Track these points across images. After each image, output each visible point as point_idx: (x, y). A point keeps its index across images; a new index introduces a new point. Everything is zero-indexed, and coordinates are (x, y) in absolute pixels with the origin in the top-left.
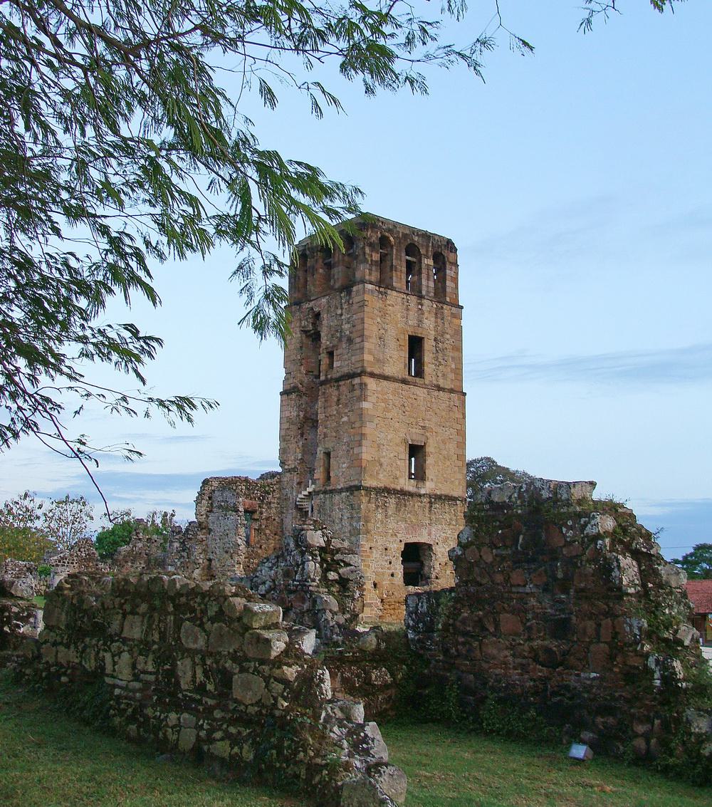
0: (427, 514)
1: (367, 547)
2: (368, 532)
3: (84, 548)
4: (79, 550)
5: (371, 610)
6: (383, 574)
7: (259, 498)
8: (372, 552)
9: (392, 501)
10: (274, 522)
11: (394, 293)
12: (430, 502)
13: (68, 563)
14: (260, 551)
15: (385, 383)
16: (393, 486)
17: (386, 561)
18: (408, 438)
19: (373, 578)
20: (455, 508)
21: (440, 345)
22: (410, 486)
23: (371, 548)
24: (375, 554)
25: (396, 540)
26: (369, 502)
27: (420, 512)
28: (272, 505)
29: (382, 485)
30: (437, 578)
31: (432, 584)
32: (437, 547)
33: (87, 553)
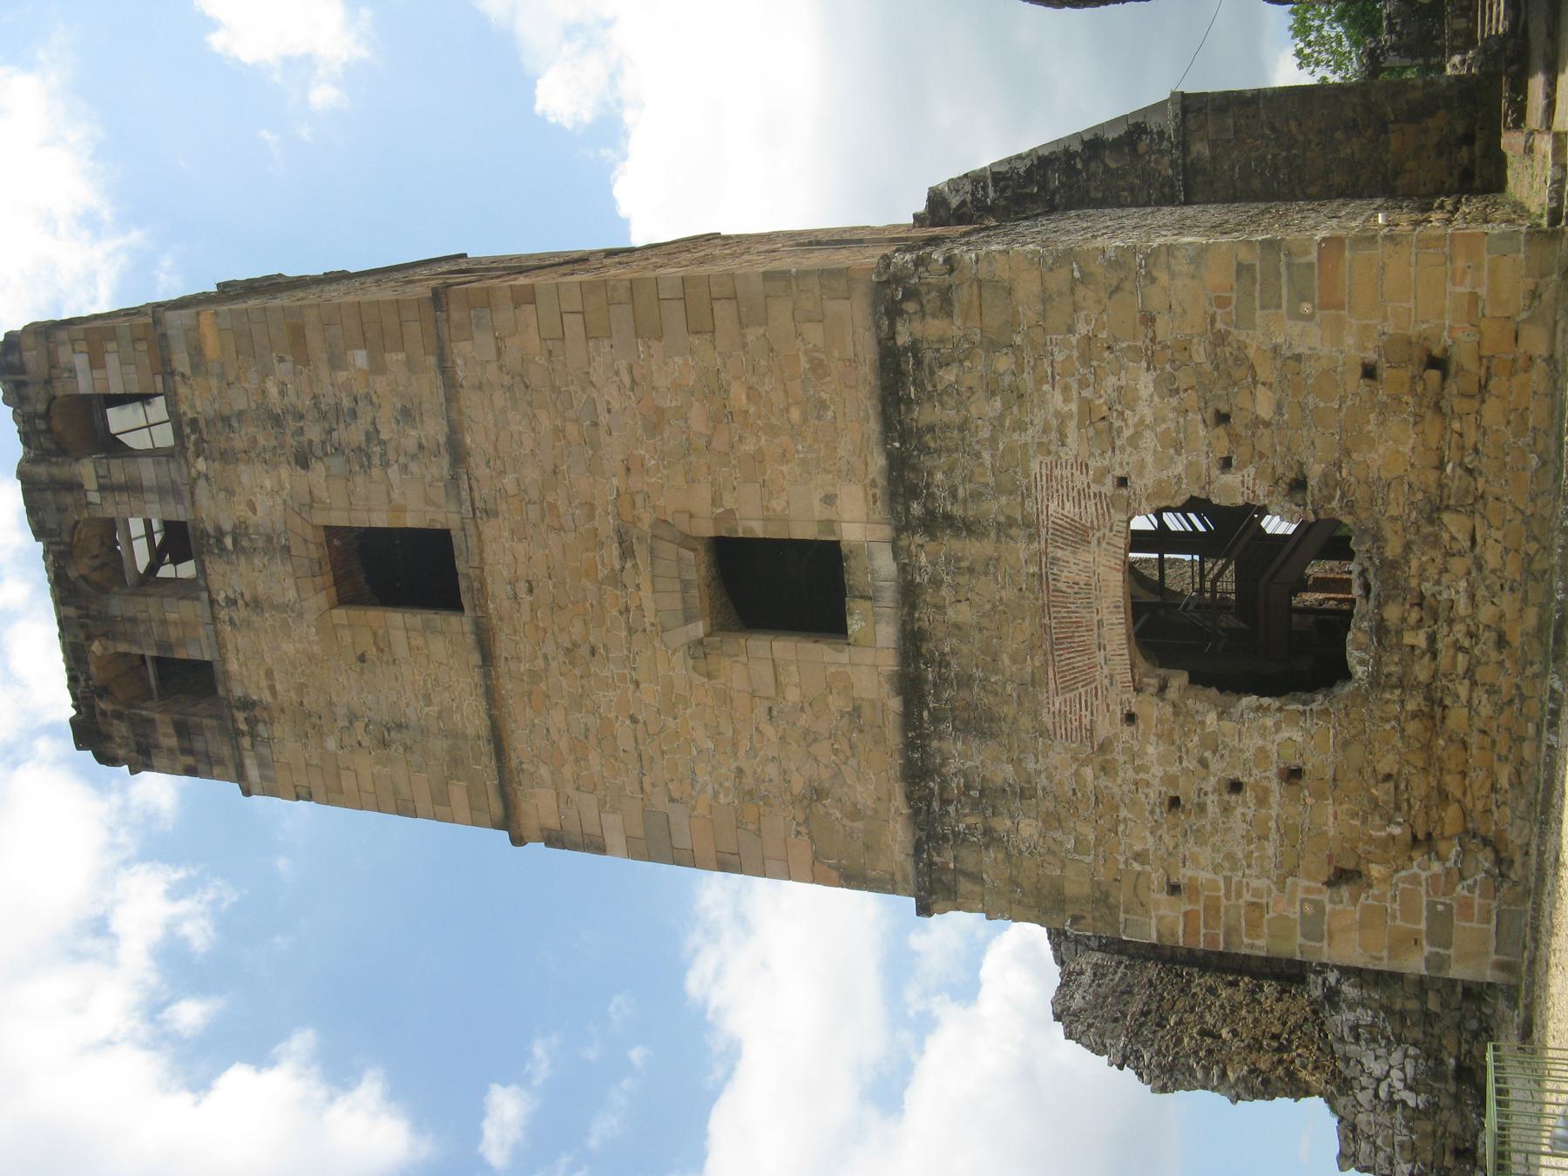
5: (1469, 918)
6: (1289, 832)
8: (1193, 890)
12: (933, 523)
15: (520, 744)
17: (1227, 810)
19: (1306, 885)
20: (929, 355)
21: (314, 433)
23: (1174, 889)
24: (1200, 871)
26: (976, 878)
29: (899, 790)
32: (1136, 483)
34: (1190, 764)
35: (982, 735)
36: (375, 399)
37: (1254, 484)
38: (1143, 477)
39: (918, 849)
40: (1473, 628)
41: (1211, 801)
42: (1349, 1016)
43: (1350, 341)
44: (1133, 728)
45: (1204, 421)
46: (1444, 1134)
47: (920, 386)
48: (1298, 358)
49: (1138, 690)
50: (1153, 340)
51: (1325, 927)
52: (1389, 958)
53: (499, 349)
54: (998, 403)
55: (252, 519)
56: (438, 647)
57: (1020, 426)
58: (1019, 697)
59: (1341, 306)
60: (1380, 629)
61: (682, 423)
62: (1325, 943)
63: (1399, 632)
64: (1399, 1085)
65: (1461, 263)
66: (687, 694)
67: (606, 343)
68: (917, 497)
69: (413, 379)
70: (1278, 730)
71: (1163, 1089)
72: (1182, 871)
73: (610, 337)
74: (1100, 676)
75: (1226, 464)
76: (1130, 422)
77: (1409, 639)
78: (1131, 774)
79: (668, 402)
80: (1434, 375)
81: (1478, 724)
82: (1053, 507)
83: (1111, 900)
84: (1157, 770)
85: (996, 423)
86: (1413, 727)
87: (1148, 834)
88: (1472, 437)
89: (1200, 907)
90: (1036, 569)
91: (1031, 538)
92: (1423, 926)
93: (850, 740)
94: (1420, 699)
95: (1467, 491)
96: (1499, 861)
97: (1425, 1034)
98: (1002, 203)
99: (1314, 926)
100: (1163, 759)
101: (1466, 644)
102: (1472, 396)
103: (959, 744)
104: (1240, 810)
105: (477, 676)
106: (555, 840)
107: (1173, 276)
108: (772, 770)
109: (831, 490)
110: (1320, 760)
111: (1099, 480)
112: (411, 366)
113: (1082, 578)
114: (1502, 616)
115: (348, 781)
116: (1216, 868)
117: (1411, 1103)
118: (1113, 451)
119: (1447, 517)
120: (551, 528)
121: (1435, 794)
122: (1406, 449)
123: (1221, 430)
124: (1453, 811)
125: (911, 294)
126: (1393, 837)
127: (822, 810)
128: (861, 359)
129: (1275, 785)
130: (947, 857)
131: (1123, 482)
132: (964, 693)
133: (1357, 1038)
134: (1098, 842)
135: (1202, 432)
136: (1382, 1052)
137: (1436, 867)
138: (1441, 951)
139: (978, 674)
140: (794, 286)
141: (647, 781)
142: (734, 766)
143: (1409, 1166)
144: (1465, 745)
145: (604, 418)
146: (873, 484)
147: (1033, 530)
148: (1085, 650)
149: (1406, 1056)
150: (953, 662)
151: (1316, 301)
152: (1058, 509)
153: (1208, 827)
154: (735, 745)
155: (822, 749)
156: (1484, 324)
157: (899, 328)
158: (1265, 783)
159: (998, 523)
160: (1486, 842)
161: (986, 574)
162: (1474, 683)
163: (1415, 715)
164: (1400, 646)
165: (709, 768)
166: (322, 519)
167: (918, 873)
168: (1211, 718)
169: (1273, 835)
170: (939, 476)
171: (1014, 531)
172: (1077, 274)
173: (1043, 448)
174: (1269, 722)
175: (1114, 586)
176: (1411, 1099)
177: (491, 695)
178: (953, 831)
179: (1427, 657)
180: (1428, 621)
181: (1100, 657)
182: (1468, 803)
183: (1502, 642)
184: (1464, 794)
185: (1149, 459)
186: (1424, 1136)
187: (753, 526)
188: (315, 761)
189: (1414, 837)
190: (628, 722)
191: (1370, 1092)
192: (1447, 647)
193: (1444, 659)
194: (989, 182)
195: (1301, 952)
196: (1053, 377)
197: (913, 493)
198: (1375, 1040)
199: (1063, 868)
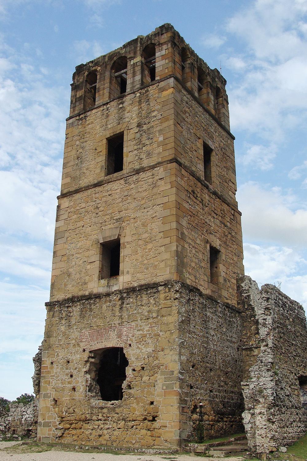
0: (118, 314)
6: (63, 389)
8: (52, 368)
9: (76, 310)
11: (94, 111)
12: (122, 298)
17: (67, 375)
19: (54, 394)
20: (156, 295)
21: (145, 127)
23: (52, 363)
24: (56, 369)
26: (53, 316)
27: (108, 314)
30: (129, 387)
32: (130, 349)
34: (76, 365)
36: (152, 144)
37: (129, 377)
38: (131, 350)
39: (58, 302)
40: (103, 429)
43: (158, 399)
44: (82, 352)
45: (142, 364)
46: (17, 427)
48: (155, 386)
49: (90, 352)
50: (158, 351)
51: (46, 399)
52: (41, 413)
53: (161, 179)
55: (126, 112)
56: (98, 170)
58: (88, 323)
60: (102, 408)
62: (43, 399)
65: (173, 424)
66: (89, 240)
68: (127, 295)
69: (156, 155)
70: (83, 385)
71: (34, 360)
74: (92, 343)
75: (134, 370)
76: (142, 346)
77: (100, 415)
79: (149, 228)
80: (151, 418)
81: (85, 431)
82: (125, 329)
85: (142, 313)
86: (83, 417)
87: (62, 356)
88: (139, 427)
90: (113, 326)
92: (47, 421)
93: (80, 282)
96: (60, 437)
98: (243, 298)
101: (100, 428)
102: (147, 428)
103: (78, 310)
104: (67, 378)
105: (92, 183)
106: (58, 207)
109: (130, 273)
111: (131, 340)
112: (159, 153)
113: (111, 337)
115: (70, 149)
116: (56, 373)
118: (136, 343)
120: (123, 199)
121: (71, 422)
122: (136, 413)
123: (140, 368)
124: (68, 426)
127: (66, 277)
128: (157, 278)
129: (72, 385)
130: (57, 308)
131: (130, 345)
132: (89, 310)
134: (61, 345)
135: (140, 364)
137: (58, 423)
138: (42, 425)
140: (173, 259)
143: (11, 420)
144: (81, 428)
145: (146, 210)
147: (120, 324)
148: (97, 339)
149: (31, 418)
151: (166, 390)
153: (64, 370)
154: (78, 253)
155: (78, 276)
157: (163, 287)
158: (72, 383)
160: (63, 434)
161: (112, 314)
162: (92, 430)
163: (86, 417)
164: (99, 413)
165: (74, 247)
166: (125, 133)
167: (53, 302)
168: (85, 370)
170: (131, 300)
171: (120, 320)
172: (172, 331)
174: (84, 383)
175: (110, 345)
176: (23, 420)
177: (87, 188)
178: (62, 310)
179: (96, 419)
180: (104, 418)
182: (71, 429)
183: (100, 436)
184: (72, 428)
185: (135, 352)
186: (17, 423)
187: (123, 253)
188: (74, 139)
189: (63, 418)
191: (24, 410)
192: (99, 424)
193: (97, 422)
194: (248, 294)
195: (41, 394)
196: (151, 327)
197: (128, 293)
198: (34, 411)
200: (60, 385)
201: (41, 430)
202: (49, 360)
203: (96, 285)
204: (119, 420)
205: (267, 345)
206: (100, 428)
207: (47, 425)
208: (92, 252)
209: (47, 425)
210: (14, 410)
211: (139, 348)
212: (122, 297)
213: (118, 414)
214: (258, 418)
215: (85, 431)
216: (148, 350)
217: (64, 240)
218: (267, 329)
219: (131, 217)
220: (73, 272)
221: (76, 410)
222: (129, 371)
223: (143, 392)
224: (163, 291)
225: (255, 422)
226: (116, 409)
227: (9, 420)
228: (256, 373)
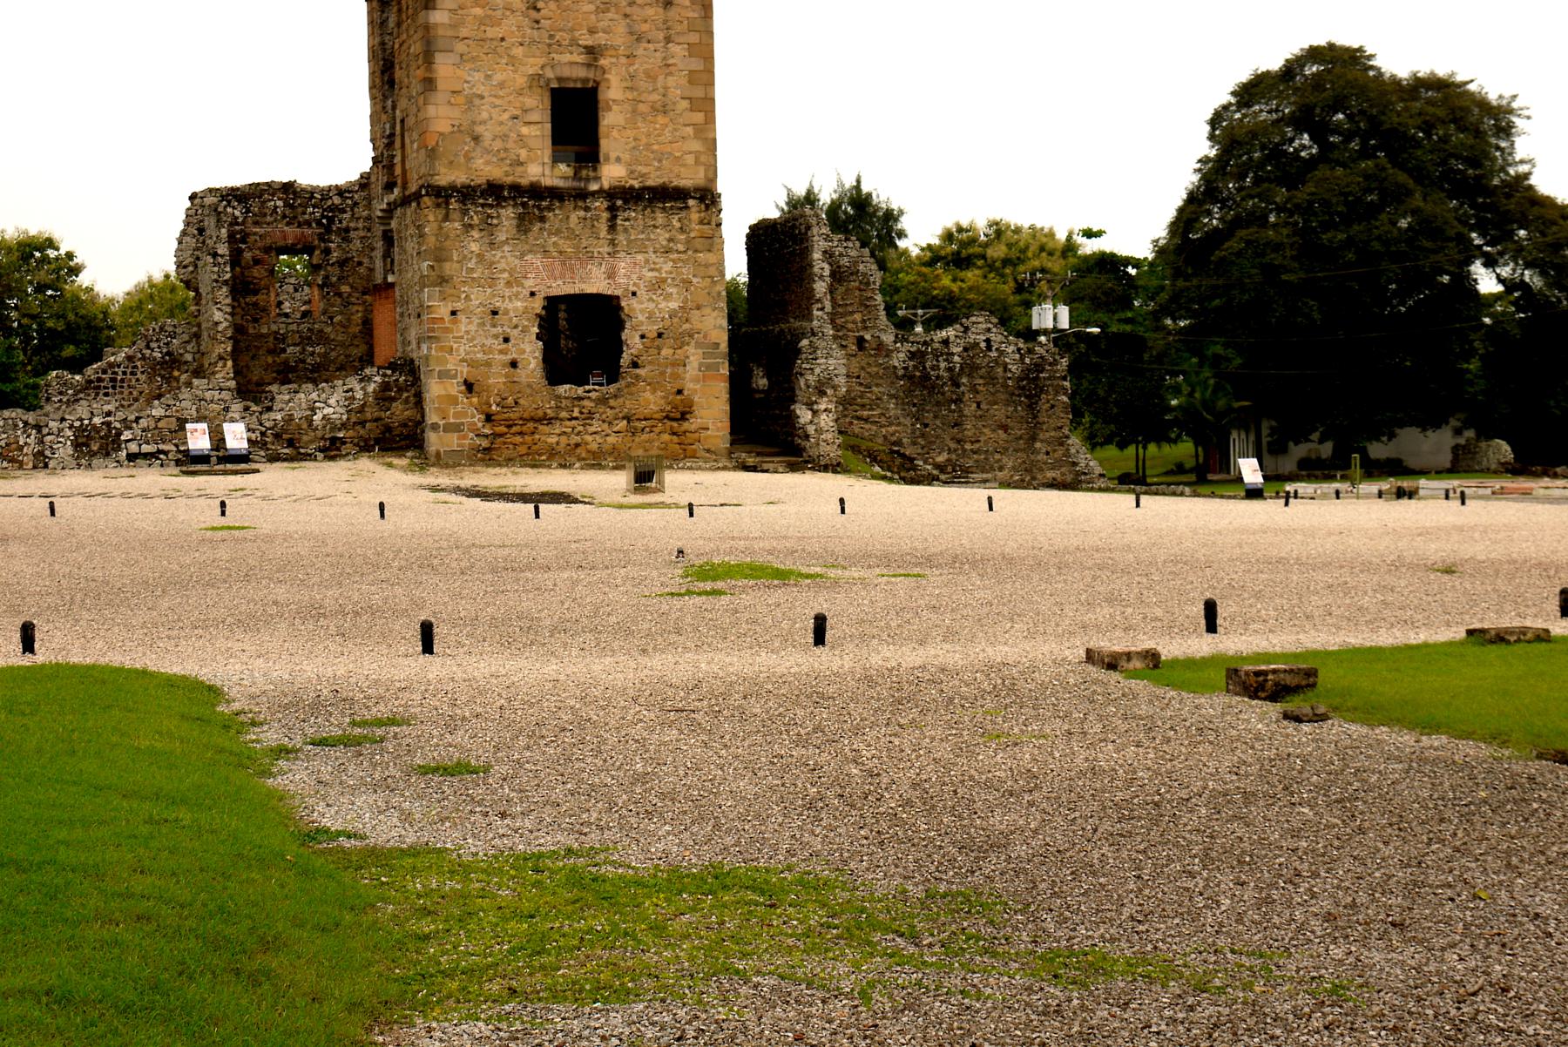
0: (603, 233)
1: (443, 311)
2: (443, 280)
3: (157, 341)
4: (148, 347)
6: (488, 364)
7: (319, 223)
8: (455, 322)
9: (508, 214)
10: (362, 270)
12: (612, 209)
13: (124, 373)
14: (329, 329)
16: (509, 180)
17: (496, 337)
18: (550, 74)
19: (464, 371)
20: (683, 214)
22: (556, 175)
23: (453, 313)
24: (464, 325)
25: (517, 295)
28: (352, 234)
29: (481, 180)
31: (623, 378)
32: (634, 302)
33: (165, 350)
35: (518, 226)
41: (499, 329)
42: (357, 387)
43: (691, 386)
47: (672, 207)
48: (685, 365)
49: (545, 298)
54: (664, 243)
57: (655, 252)
59: (704, 381)
60: (580, 399)
61: (651, 89)
63: (579, 406)
64: (325, 412)
65: (719, 424)
67: (687, 54)
70: (536, 358)
72: (464, 317)
73: (690, 56)
75: (643, 337)
77: (576, 410)
78: (507, 294)
81: (543, 438)
82: (623, 264)
83: (444, 284)
84: (510, 306)
86: (540, 413)
88: (657, 430)
89: (447, 325)
91: (609, 254)
92: (452, 421)
94: (552, 415)
95: (636, 429)
96: (485, 449)
97: (354, 423)
99: (444, 375)
100: (516, 309)
101: (576, 431)
107: (715, 318)
108: (485, 115)
110: (522, 375)
111: (635, 284)
113: (593, 275)
114: (587, 444)
116: (467, 332)
117: (315, 417)
119: (625, 422)
120: (598, 8)
122: (652, 406)
123: (656, 335)
124: (503, 429)
125: (707, 207)
126: (491, 406)
129: (509, 357)
130: (454, 204)
131: (634, 294)
133: (347, 392)
136: (341, 403)
137: (480, 425)
139: (547, 226)
141: (470, 42)
142: (486, 94)
144: (533, 433)
146: (626, 182)
150: (550, 214)
152: (623, 266)
154: (495, 96)
155: (498, 145)
156: (697, 434)
159: (613, 240)
164: (573, 406)
169: (486, 357)
170: (633, 214)
173: (647, 261)
174: (537, 354)
180: (583, 416)
181: (560, 282)
182: (508, 436)
183: (577, 445)
184: (513, 434)
185: (643, 306)
190: (500, 36)
191: (317, 399)
193: (568, 423)
197: (626, 201)
199: (458, 262)
200: (478, 355)
201: (440, 438)
202: (447, 306)
203: (547, 172)
204: (616, 419)
205: (822, 309)
206: (576, 431)
207: (456, 428)
208: (530, 102)
209: (456, 428)
210: (287, 397)
211: (653, 301)
212: (614, 204)
213: (612, 408)
214: (822, 417)
215: (543, 438)
216: (670, 305)
217: (452, 58)
218: (824, 284)
219: (620, 52)
220: (486, 133)
221: (521, 401)
222: (632, 340)
223: (663, 373)
224: (698, 209)
225: (819, 423)
226: (610, 401)
227: (275, 420)
228: (825, 351)
